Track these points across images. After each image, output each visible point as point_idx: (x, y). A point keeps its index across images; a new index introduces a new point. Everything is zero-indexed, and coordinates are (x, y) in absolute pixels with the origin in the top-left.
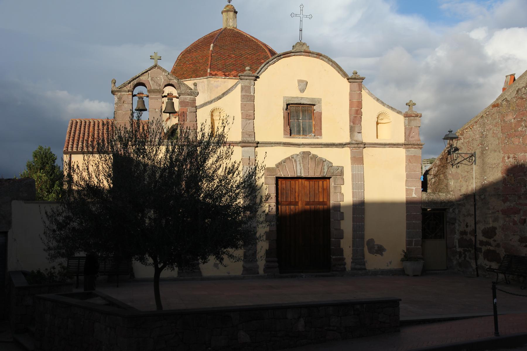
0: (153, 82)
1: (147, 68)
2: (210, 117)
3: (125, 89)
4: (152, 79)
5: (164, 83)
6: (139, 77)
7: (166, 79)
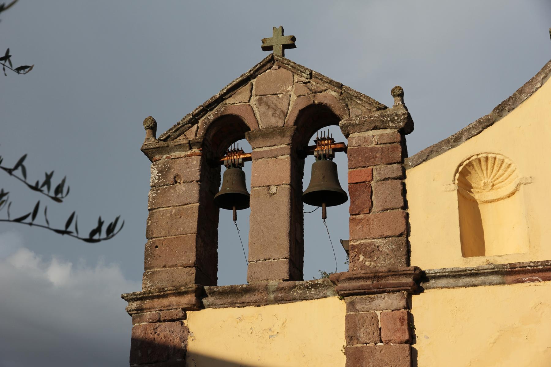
0: (263, 108)
1: (246, 71)
2: (454, 187)
3: (182, 140)
4: (260, 101)
5: (296, 104)
6: (221, 99)
7: (304, 90)
